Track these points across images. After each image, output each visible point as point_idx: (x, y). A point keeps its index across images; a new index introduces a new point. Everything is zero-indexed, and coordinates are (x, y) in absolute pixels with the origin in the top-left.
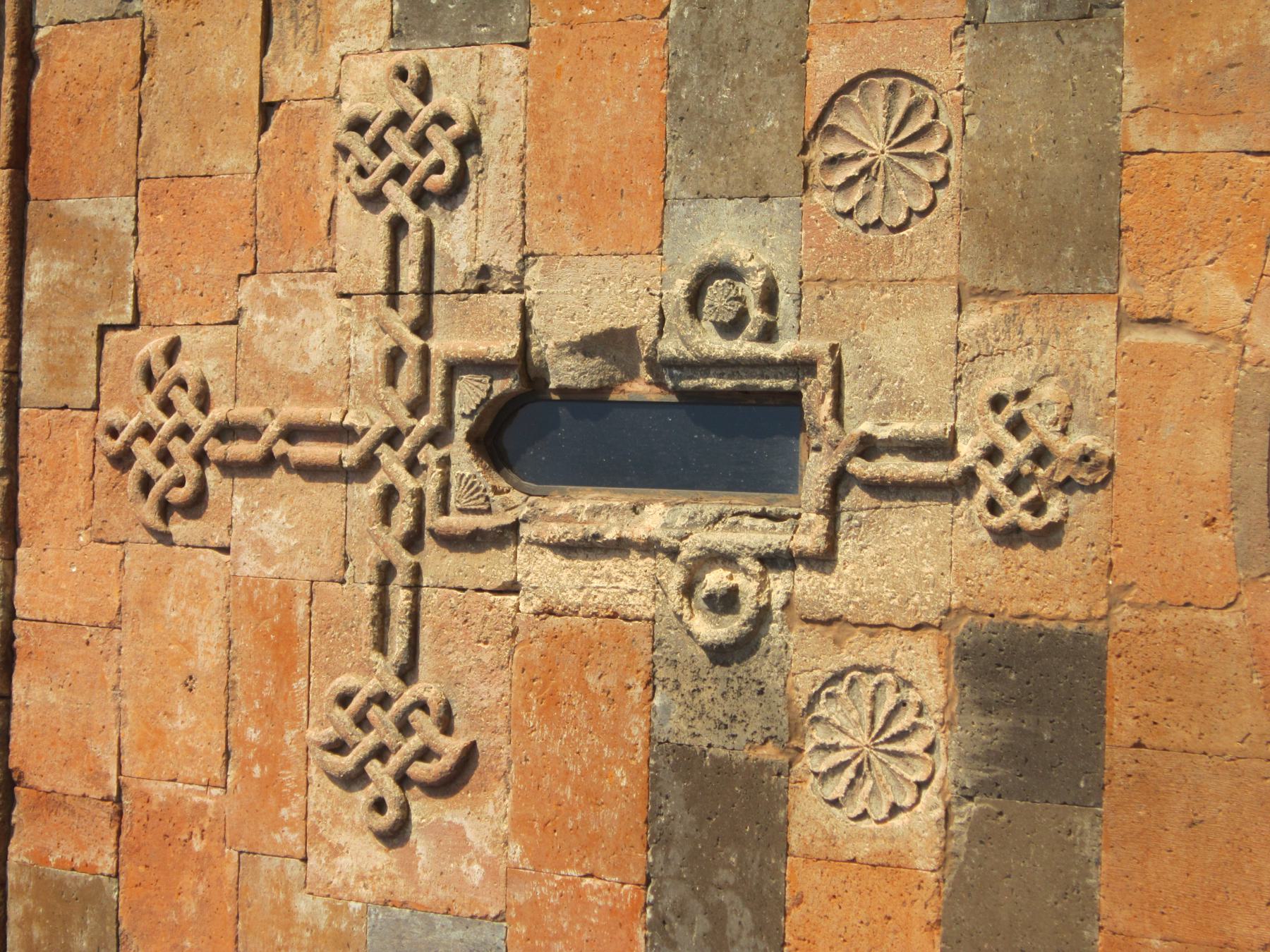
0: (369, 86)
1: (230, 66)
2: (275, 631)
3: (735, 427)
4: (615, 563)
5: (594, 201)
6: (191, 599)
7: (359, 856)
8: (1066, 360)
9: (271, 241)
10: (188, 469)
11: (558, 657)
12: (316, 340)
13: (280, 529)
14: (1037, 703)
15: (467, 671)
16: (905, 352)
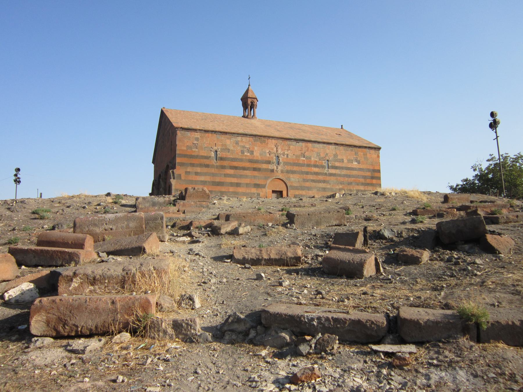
0: (286, 153)
1: (286, 148)
2: (272, 149)
3: (278, 163)
4: (274, 159)
5: (283, 160)
6: (273, 146)
7: (267, 152)
8: (279, 172)
9: (282, 150)
10: (277, 146)
11: (272, 158)
12: (280, 151)
13: (275, 149)
14: (272, 171)
15: (272, 155)
16: (280, 168)
